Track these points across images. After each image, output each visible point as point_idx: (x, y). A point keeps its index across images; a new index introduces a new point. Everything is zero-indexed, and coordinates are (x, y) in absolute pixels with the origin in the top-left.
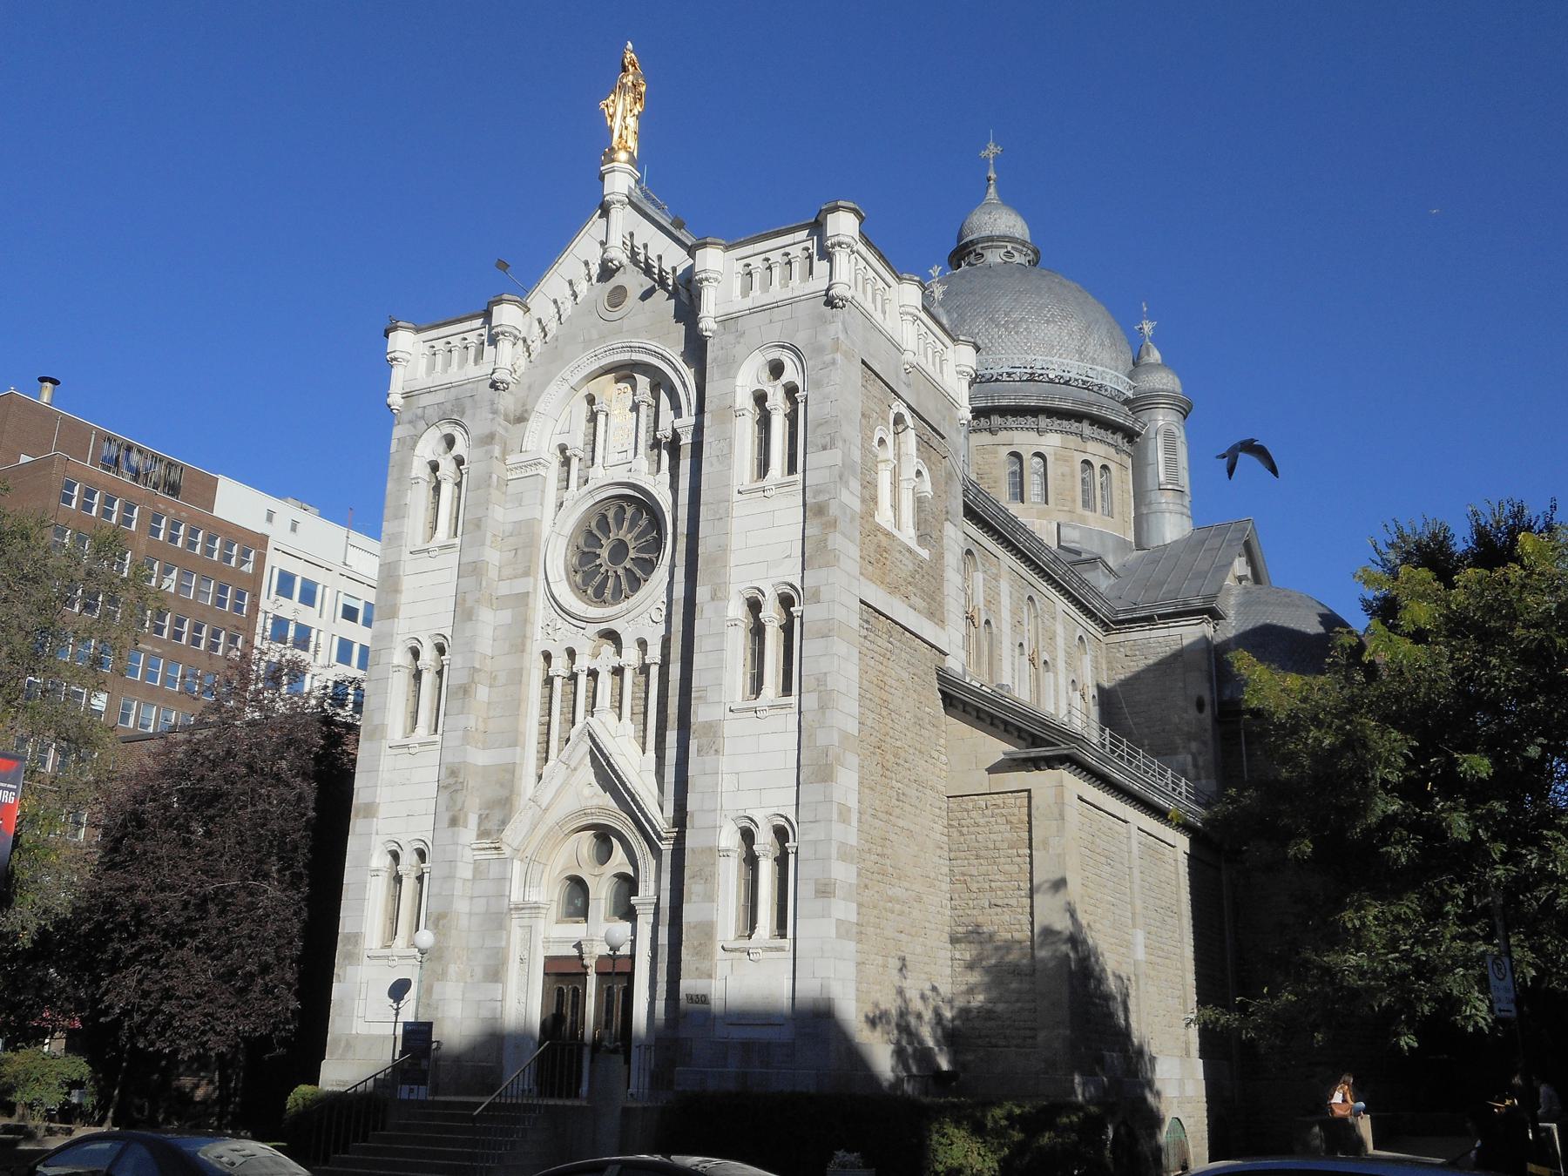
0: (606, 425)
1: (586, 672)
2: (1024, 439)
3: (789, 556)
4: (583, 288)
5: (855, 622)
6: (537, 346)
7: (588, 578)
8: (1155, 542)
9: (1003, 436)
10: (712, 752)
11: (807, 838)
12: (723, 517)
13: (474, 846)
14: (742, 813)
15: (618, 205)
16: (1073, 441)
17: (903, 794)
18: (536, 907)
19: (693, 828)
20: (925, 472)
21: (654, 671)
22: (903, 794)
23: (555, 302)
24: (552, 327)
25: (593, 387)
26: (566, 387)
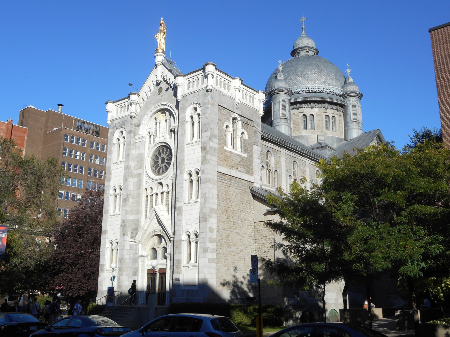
0: (160, 126)
1: (155, 194)
2: (307, 110)
4: (152, 88)
5: (216, 178)
6: (142, 105)
7: (156, 167)
8: (350, 138)
9: (301, 110)
12: (183, 152)
13: (129, 241)
14: (187, 231)
15: (159, 65)
16: (322, 110)
17: (236, 223)
18: (144, 256)
19: (176, 235)
20: (246, 132)
21: (170, 193)
22: (236, 223)
23: (146, 93)
24: (146, 99)
25: (156, 116)
26: (149, 116)
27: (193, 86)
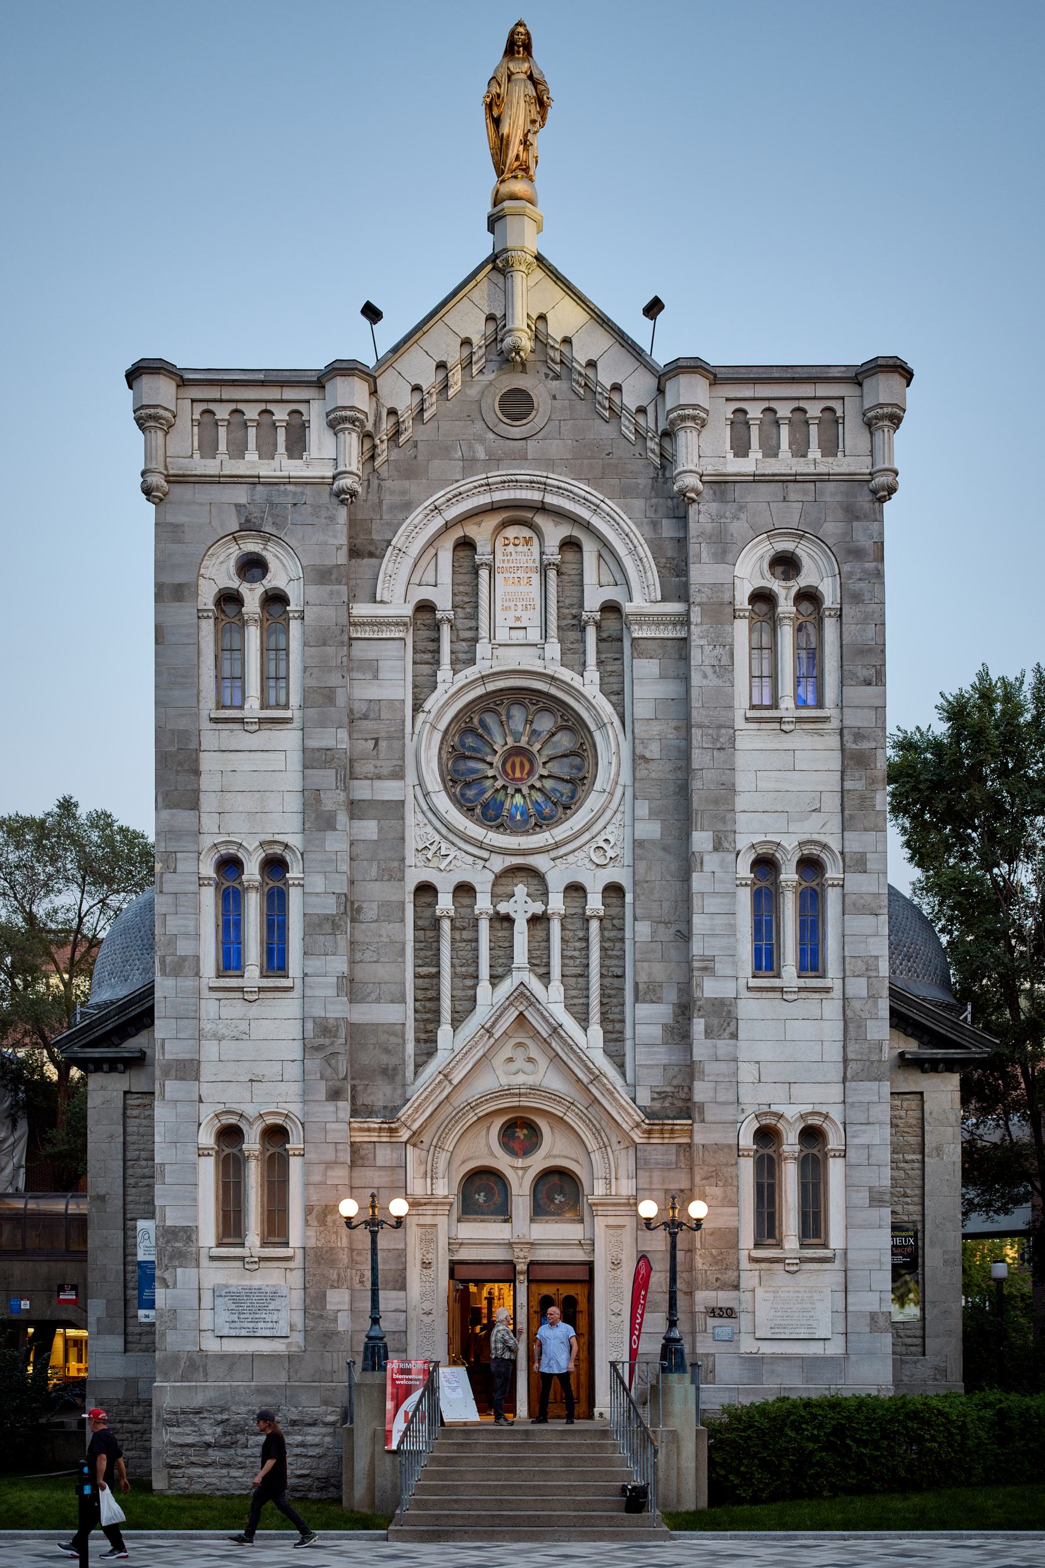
3: (817, 810)
10: (726, 1035)
11: (856, 1141)
14: (765, 1109)
19: (703, 1121)
27: (771, 451)
